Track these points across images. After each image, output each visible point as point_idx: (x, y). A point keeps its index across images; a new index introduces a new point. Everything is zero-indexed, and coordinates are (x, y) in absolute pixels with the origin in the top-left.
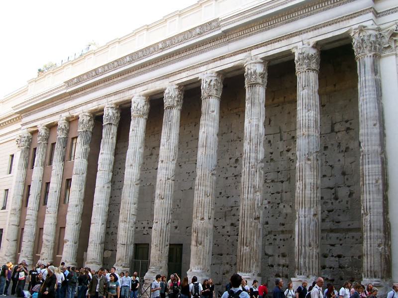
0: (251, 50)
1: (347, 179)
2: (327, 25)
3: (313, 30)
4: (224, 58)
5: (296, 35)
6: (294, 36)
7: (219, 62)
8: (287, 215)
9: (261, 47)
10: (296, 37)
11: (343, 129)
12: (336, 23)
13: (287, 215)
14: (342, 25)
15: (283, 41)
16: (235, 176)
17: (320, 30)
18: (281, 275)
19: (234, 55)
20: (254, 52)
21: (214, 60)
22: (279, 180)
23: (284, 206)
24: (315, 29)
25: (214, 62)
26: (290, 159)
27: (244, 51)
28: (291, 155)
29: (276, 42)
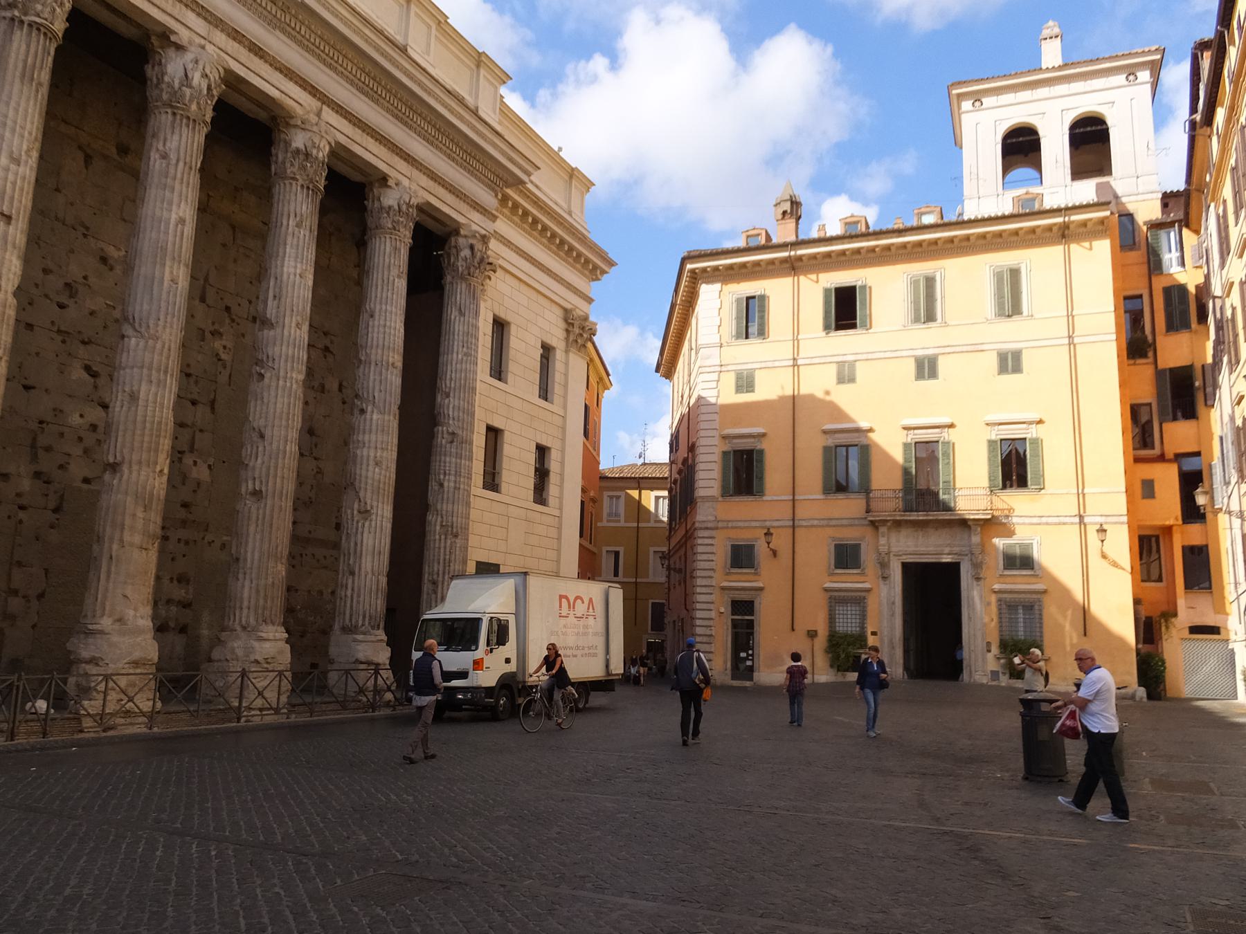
0: (323, 103)
1: (316, 446)
2: (447, 189)
3: (428, 176)
4: (261, 58)
5: (405, 160)
6: (401, 157)
7: (241, 48)
8: (199, 484)
9: (346, 118)
10: (402, 162)
11: (320, 346)
12: (457, 196)
13: (199, 484)
14: (464, 207)
15: (382, 147)
16: (59, 331)
17: (436, 185)
18: (172, 624)
19: (286, 76)
20: (329, 115)
21: (236, 35)
22: (189, 396)
23: (195, 463)
24: (432, 179)
25: (234, 39)
26: (217, 355)
27: (313, 91)
28: (221, 349)
29: (372, 137)
